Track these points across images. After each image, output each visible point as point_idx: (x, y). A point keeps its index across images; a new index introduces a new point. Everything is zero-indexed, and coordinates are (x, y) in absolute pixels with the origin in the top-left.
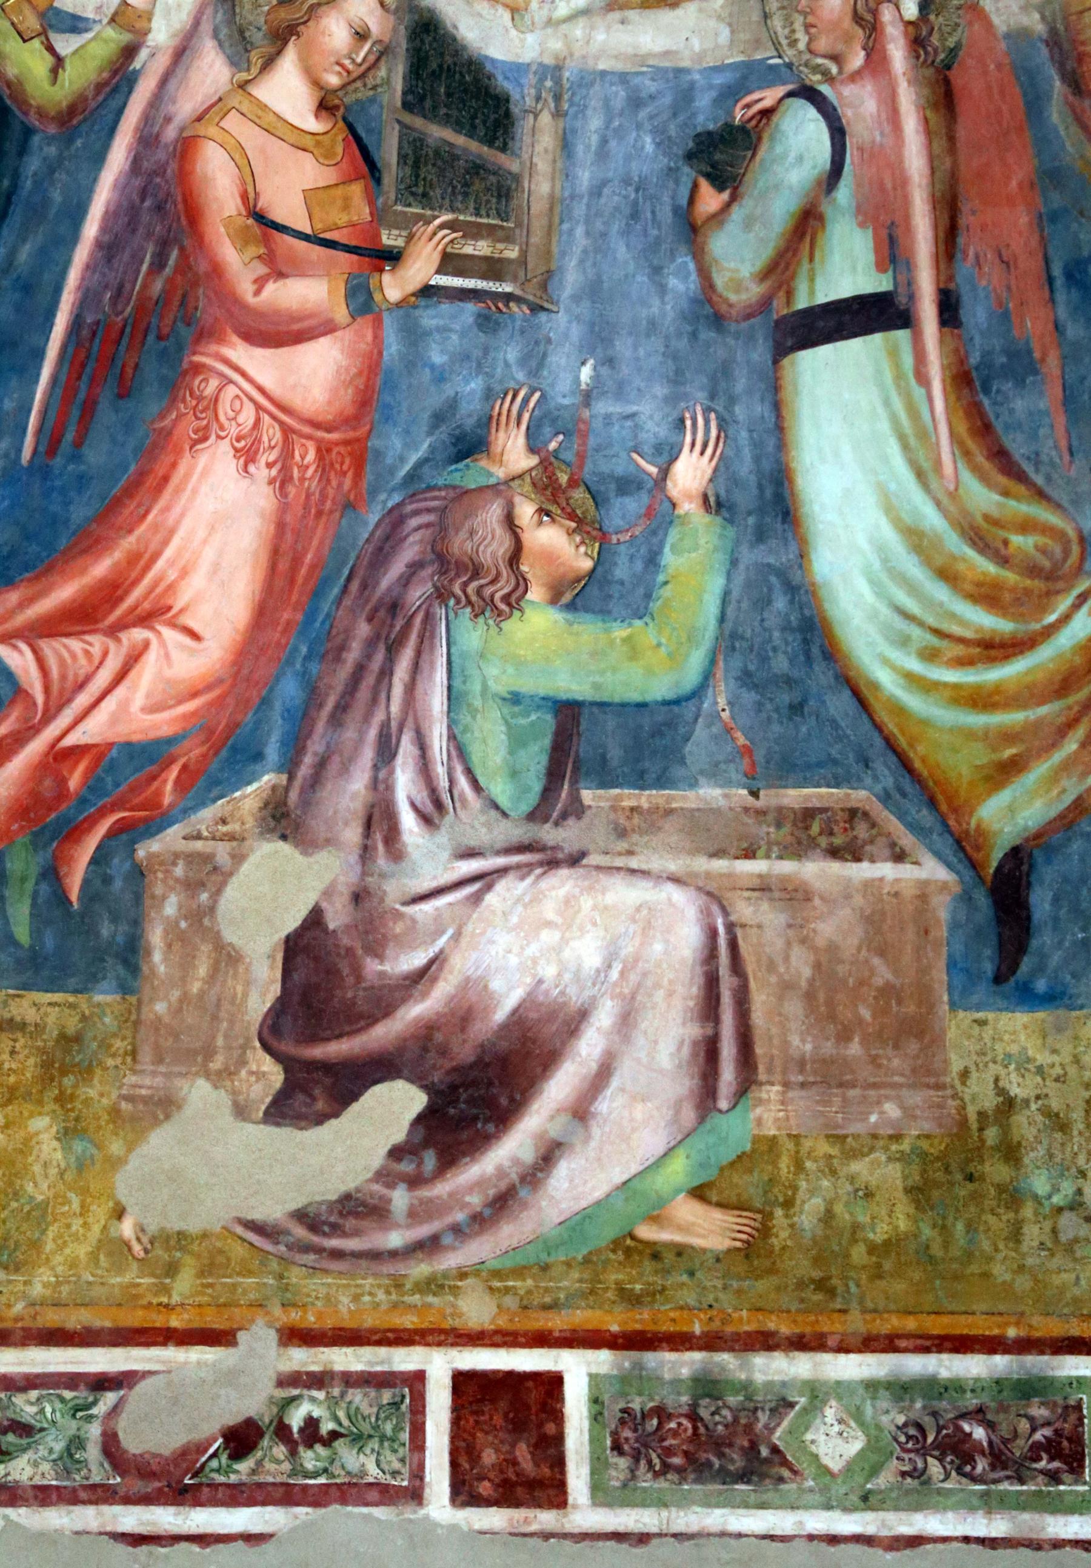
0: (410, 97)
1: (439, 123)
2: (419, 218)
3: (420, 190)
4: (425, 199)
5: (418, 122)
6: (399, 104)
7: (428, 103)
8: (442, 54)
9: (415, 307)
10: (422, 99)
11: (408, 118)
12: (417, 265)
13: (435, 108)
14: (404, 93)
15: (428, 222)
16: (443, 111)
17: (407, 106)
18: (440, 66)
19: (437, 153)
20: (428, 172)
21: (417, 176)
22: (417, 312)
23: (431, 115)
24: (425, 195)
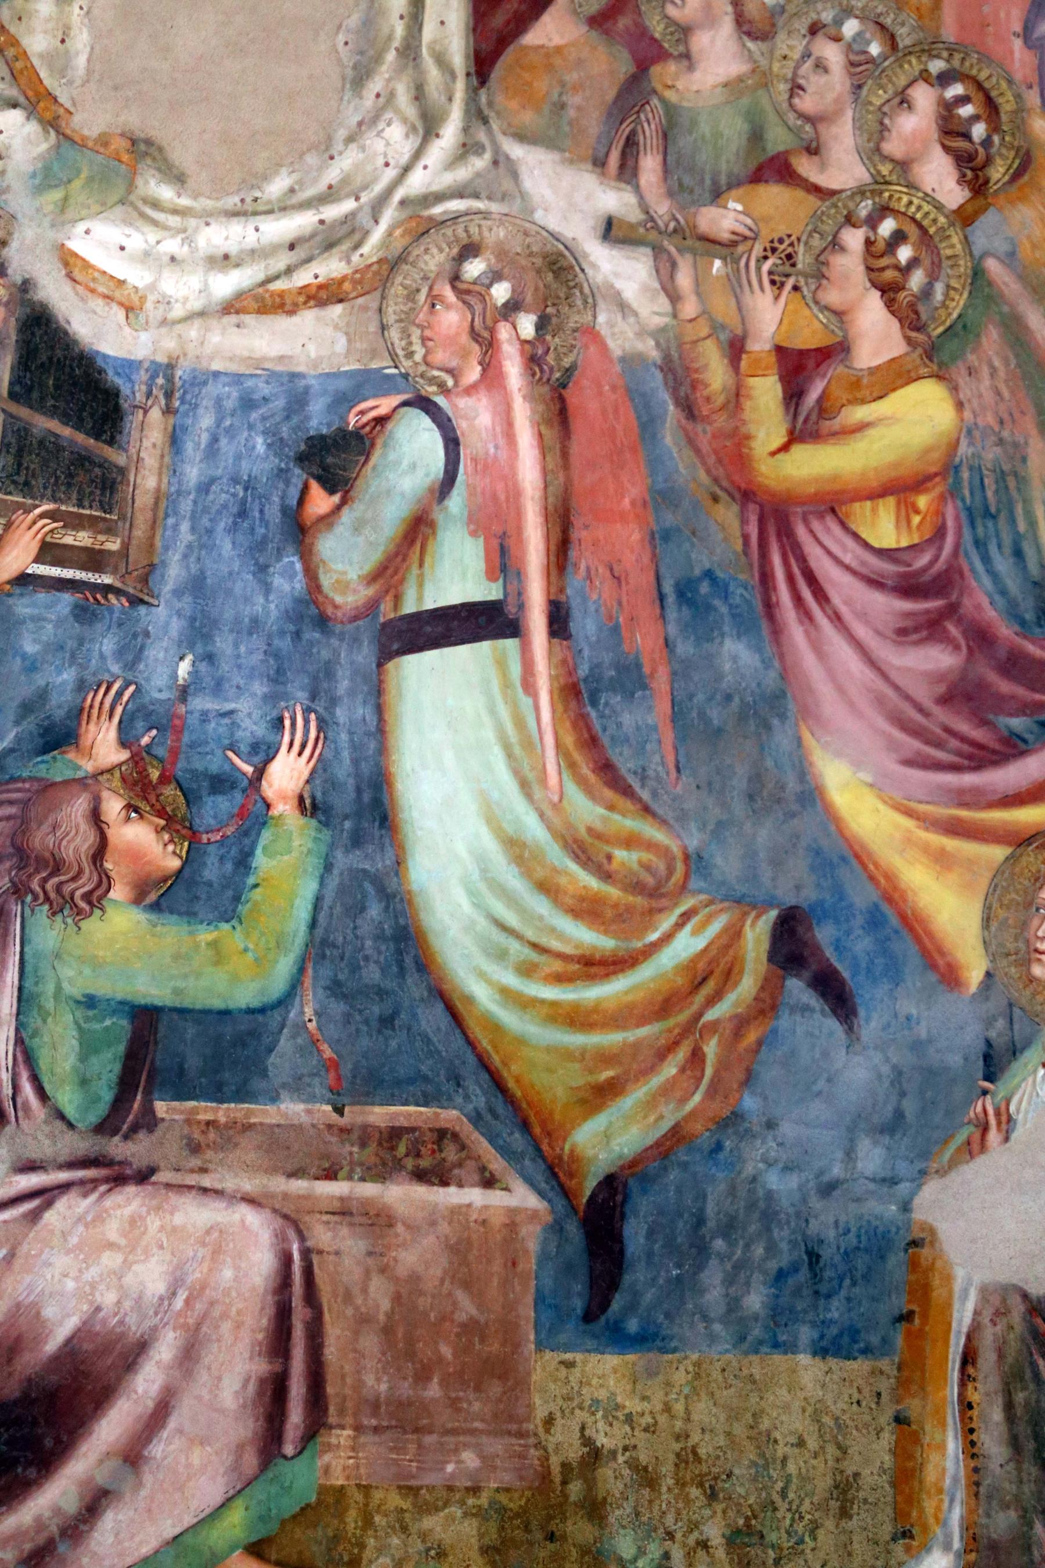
0: (17, 388)
1: (44, 414)
2: (19, 506)
3: (21, 479)
4: (26, 488)
5: (23, 412)
6: (5, 393)
7: (35, 395)
8: (52, 348)
9: (9, 595)
10: (30, 390)
11: (14, 408)
12: (14, 553)
13: (42, 399)
14: (11, 384)
15: (27, 511)
16: (50, 402)
17: (13, 396)
18: (50, 359)
19: (41, 443)
20: (32, 461)
21: (20, 465)
22: (11, 601)
23: (39, 407)
24: (26, 483)
